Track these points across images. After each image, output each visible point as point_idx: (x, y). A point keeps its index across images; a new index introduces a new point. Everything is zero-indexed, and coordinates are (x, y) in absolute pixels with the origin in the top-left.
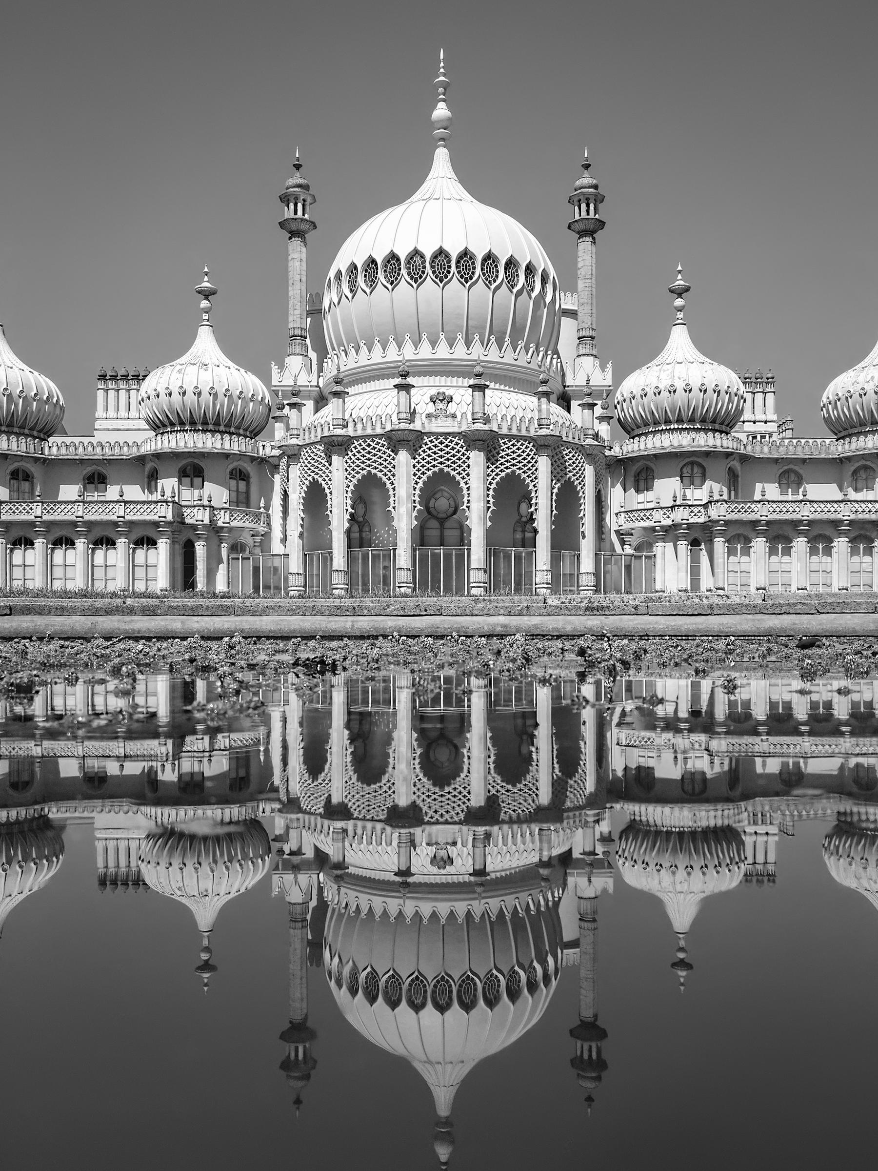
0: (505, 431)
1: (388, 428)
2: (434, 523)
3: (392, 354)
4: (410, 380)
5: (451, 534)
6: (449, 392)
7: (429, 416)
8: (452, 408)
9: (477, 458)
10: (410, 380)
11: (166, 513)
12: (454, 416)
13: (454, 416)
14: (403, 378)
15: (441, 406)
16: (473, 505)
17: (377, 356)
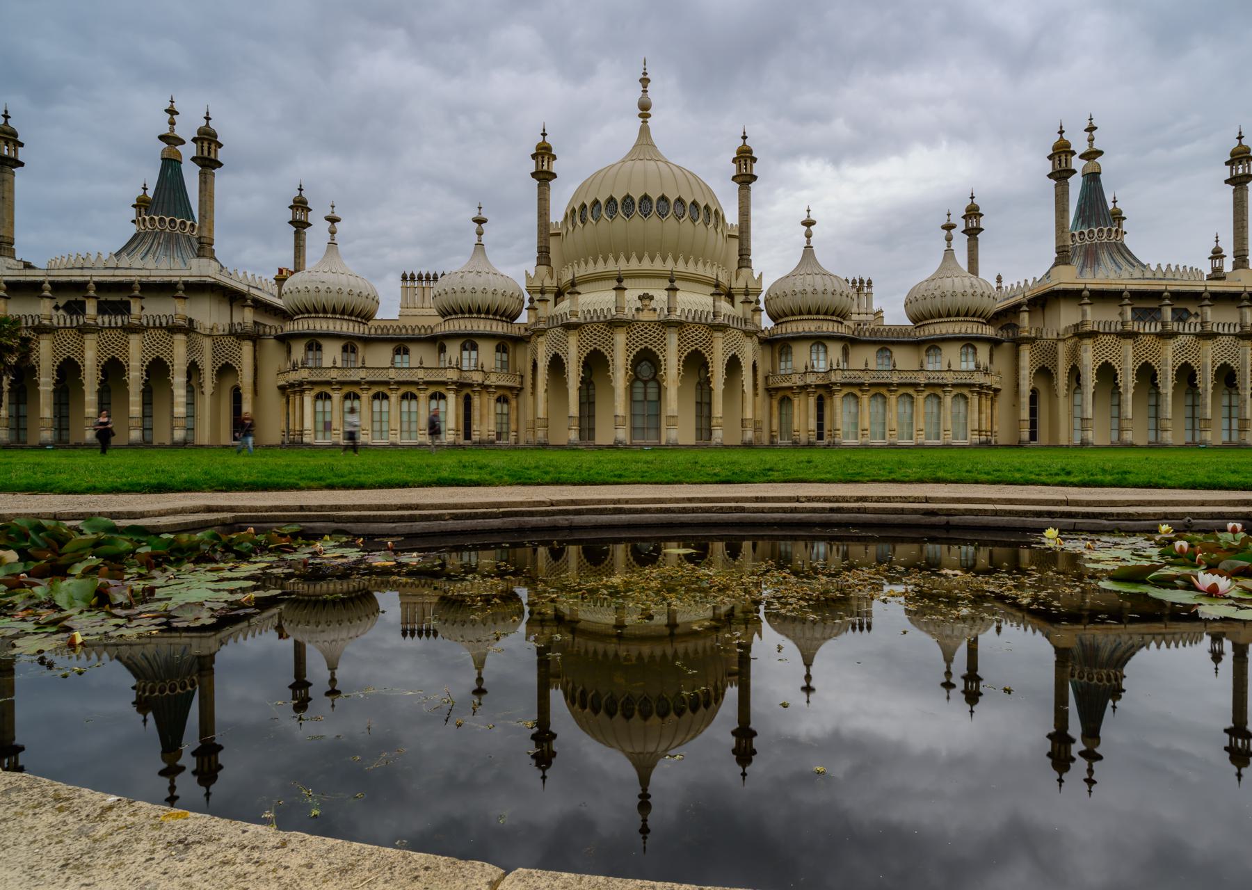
0: (690, 320)
1: (609, 317)
2: (639, 384)
3: (611, 267)
4: (624, 284)
5: (652, 392)
6: (651, 293)
7: (638, 309)
8: (653, 304)
9: (673, 340)
10: (624, 284)
11: (452, 375)
12: (655, 310)
13: (655, 310)
14: (620, 283)
15: (647, 302)
16: (668, 372)
17: (601, 267)
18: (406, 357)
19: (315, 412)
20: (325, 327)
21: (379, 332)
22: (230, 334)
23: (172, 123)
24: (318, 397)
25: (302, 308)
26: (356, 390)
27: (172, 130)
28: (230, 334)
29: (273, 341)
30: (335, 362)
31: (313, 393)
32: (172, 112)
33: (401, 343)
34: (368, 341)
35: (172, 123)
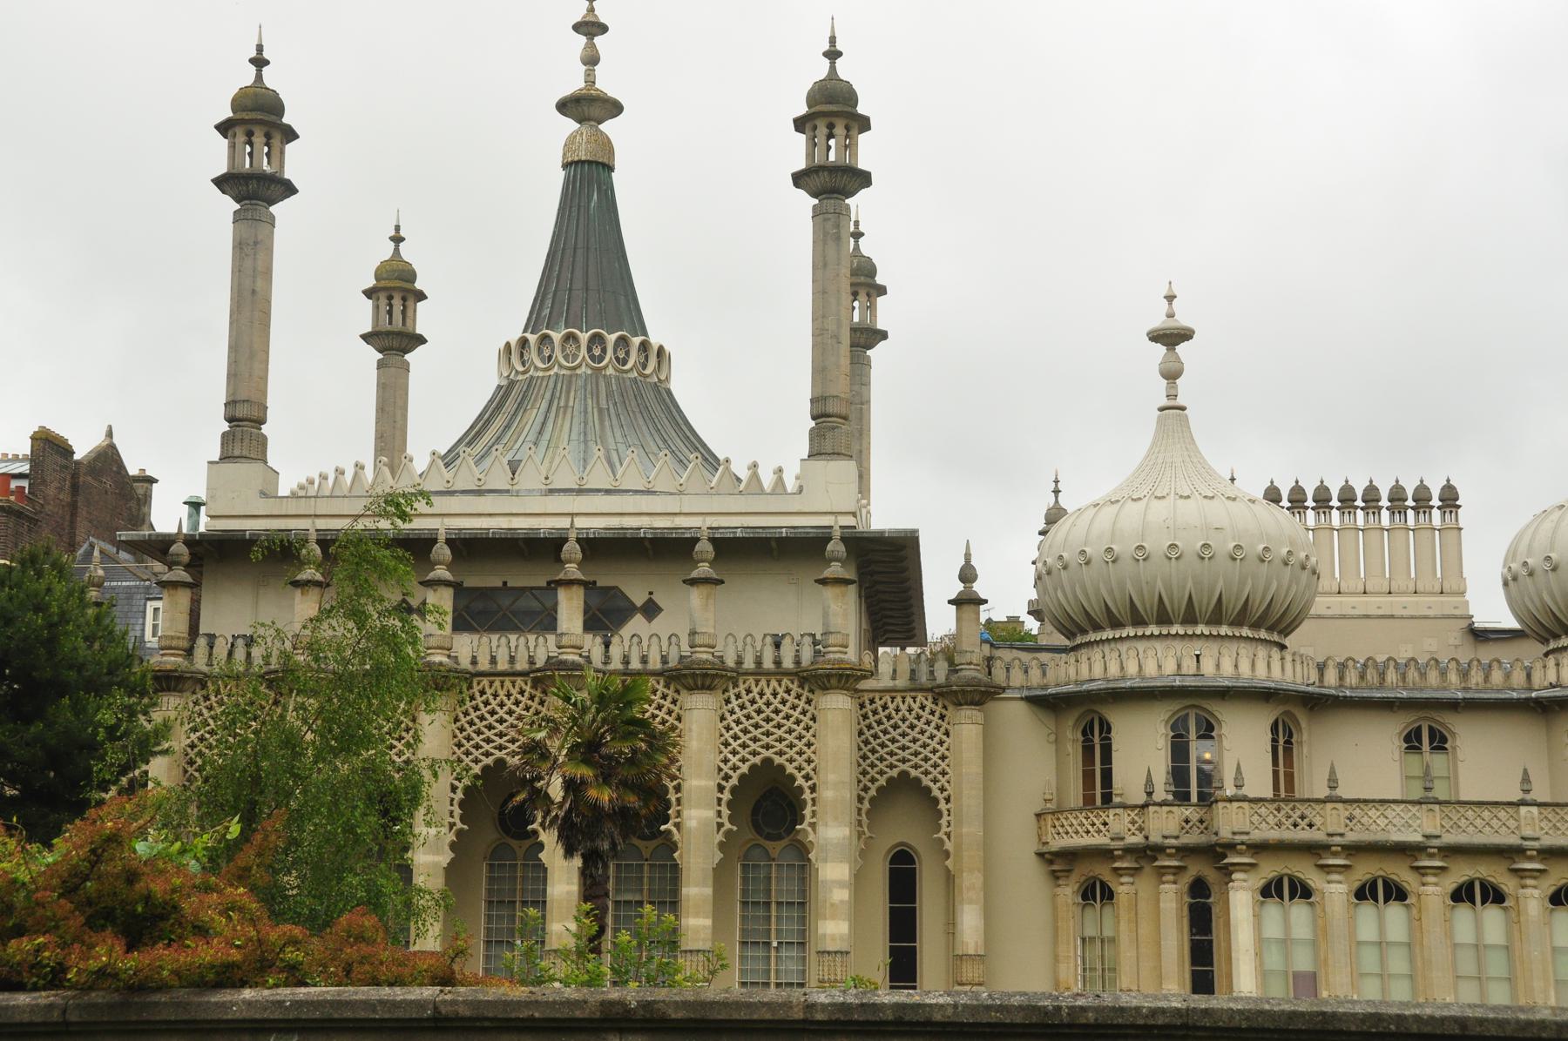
18: (1438, 762)
19: (1260, 942)
20: (1170, 667)
21: (1352, 678)
22: (915, 688)
23: (591, 60)
24: (1271, 891)
25: (1097, 613)
26: (1401, 873)
27: (590, 80)
28: (915, 688)
29: (1022, 706)
30: (1333, 783)
31: (1257, 880)
32: (591, 28)
33: (1427, 722)
34: (1317, 704)
35: (591, 60)
